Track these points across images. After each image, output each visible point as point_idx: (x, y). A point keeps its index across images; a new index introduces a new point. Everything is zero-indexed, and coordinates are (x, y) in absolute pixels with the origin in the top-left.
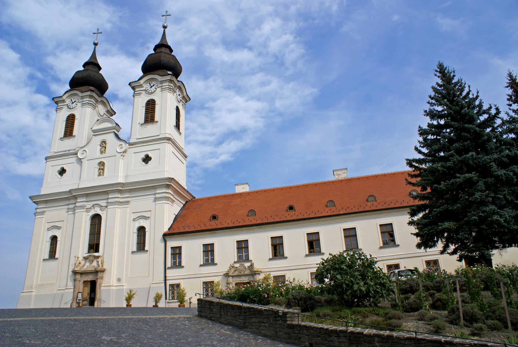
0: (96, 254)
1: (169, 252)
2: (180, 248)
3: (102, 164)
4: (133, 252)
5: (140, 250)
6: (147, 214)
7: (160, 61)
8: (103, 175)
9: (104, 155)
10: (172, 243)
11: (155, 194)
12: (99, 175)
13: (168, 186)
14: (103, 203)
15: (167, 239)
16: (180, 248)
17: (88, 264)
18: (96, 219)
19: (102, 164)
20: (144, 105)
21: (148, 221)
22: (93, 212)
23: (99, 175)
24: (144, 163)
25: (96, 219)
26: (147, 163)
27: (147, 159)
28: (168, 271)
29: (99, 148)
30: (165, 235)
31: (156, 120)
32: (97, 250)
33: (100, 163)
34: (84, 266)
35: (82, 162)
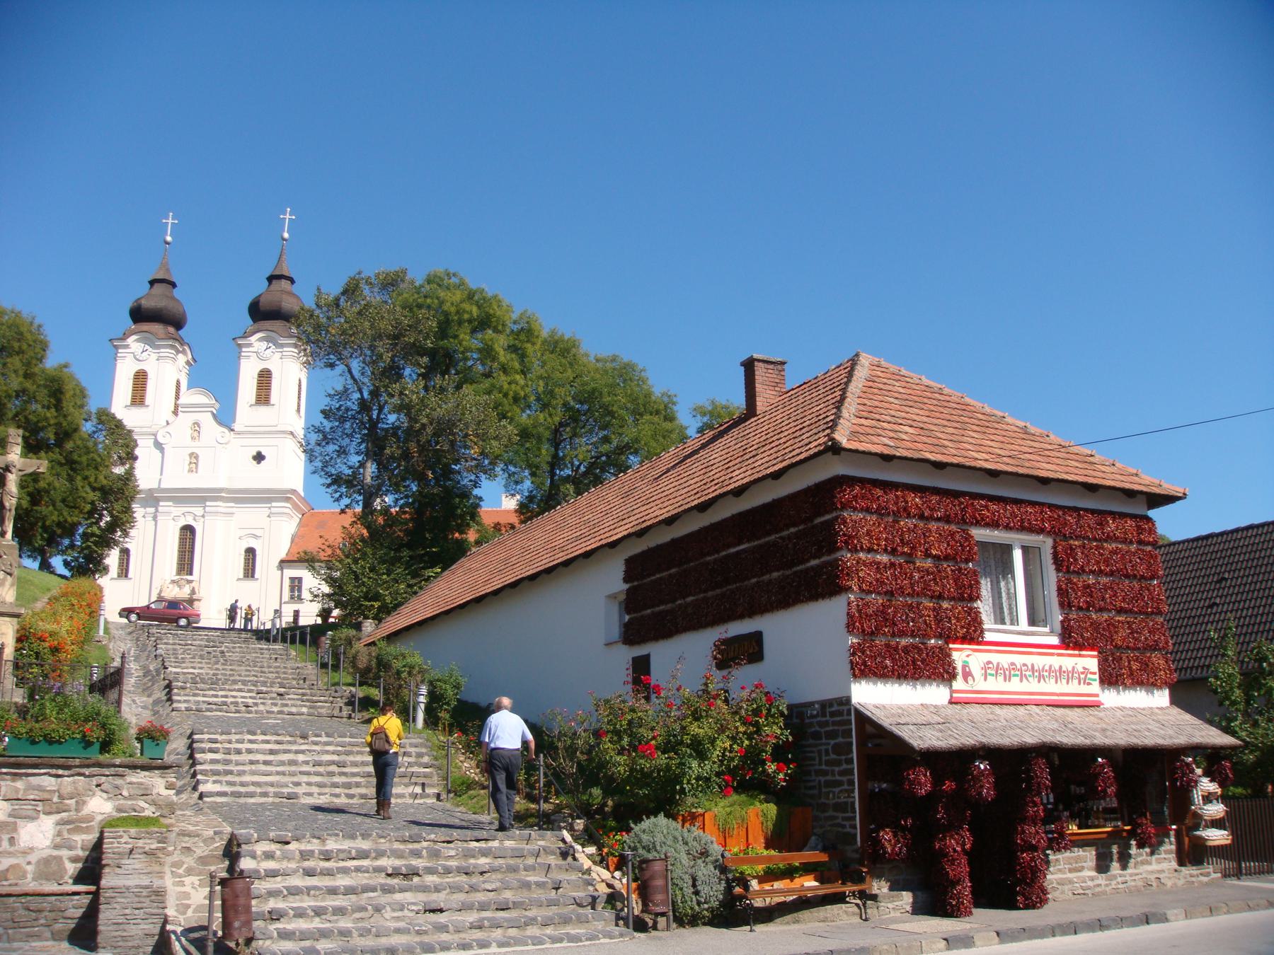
0: (189, 578)
1: (287, 583)
2: (300, 579)
3: (194, 456)
4: (239, 579)
5: (248, 577)
6: (258, 533)
7: (281, 308)
8: (196, 472)
9: (196, 443)
10: (290, 573)
11: (270, 508)
12: (190, 471)
13: (287, 499)
14: (198, 511)
15: (283, 564)
16: (300, 579)
17: (177, 589)
18: (188, 533)
19: (194, 456)
20: (256, 376)
21: (260, 541)
22: (183, 522)
23: (190, 471)
24: (255, 462)
25: (188, 533)
26: (259, 463)
27: (259, 457)
28: (283, 605)
29: (189, 432)
30: (282, 562)
31: (272, 402)
32: (191, 573)
33: (192, 454)
34: (171, 591)
35: (163, 449)
